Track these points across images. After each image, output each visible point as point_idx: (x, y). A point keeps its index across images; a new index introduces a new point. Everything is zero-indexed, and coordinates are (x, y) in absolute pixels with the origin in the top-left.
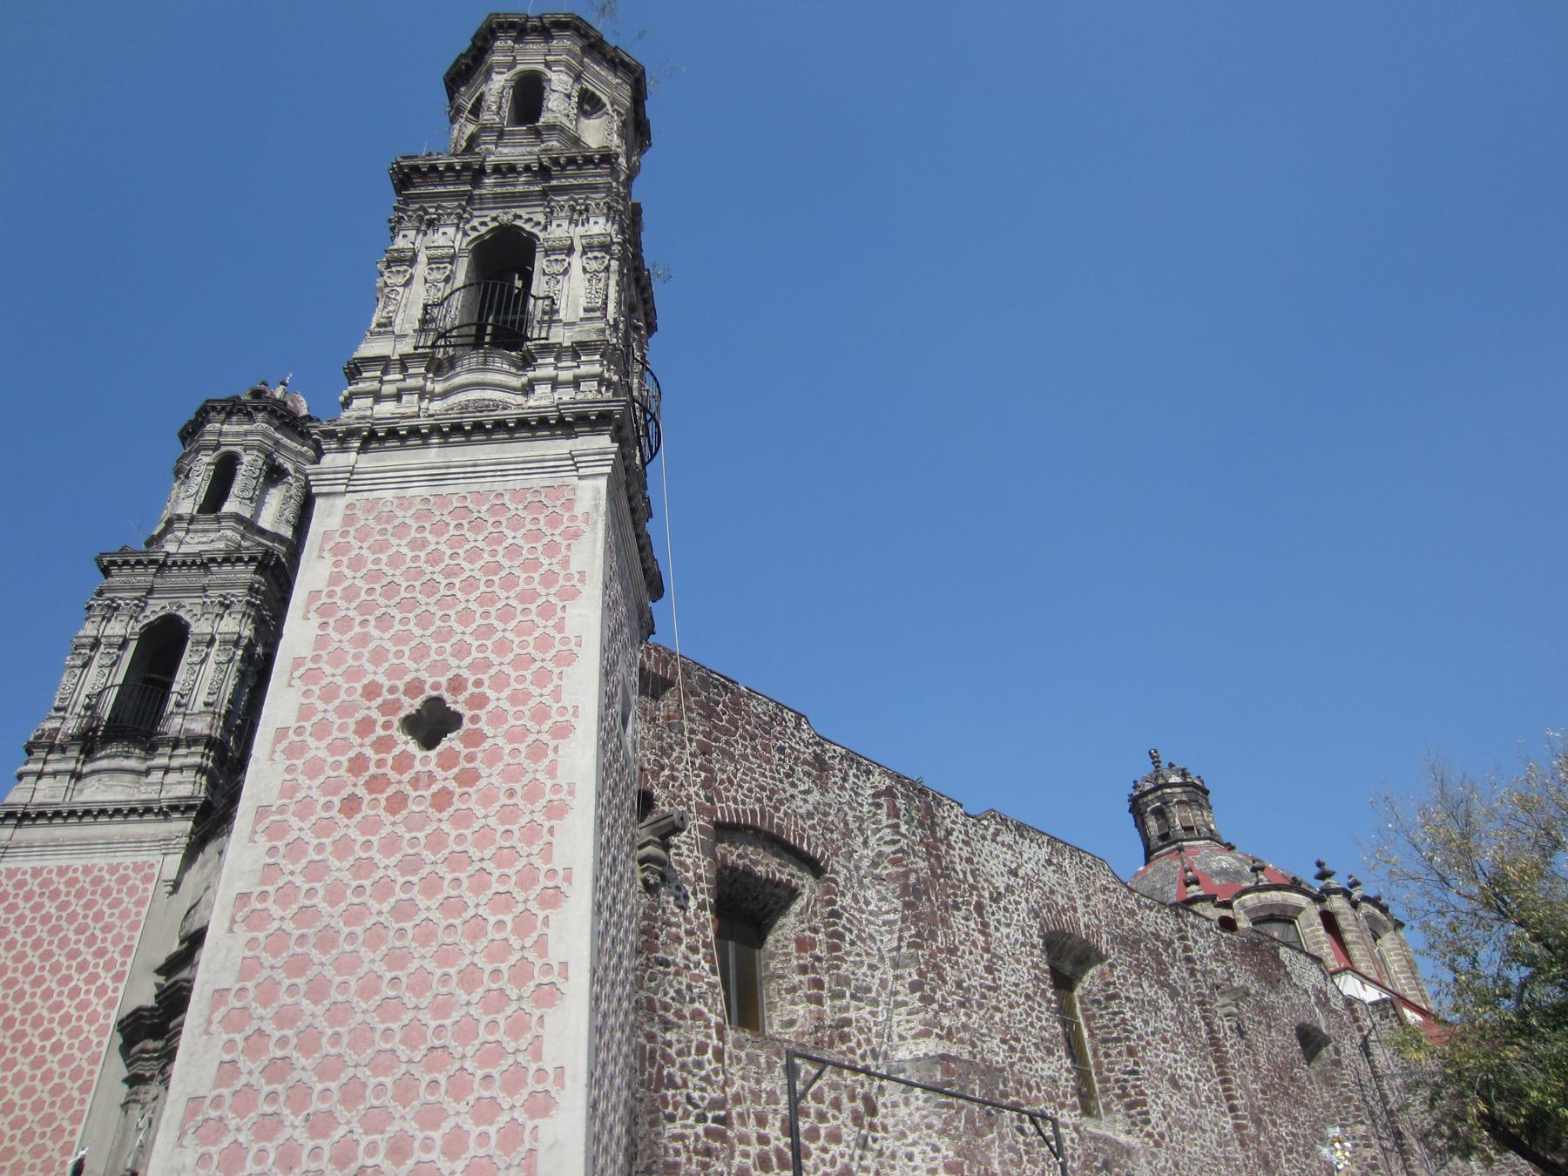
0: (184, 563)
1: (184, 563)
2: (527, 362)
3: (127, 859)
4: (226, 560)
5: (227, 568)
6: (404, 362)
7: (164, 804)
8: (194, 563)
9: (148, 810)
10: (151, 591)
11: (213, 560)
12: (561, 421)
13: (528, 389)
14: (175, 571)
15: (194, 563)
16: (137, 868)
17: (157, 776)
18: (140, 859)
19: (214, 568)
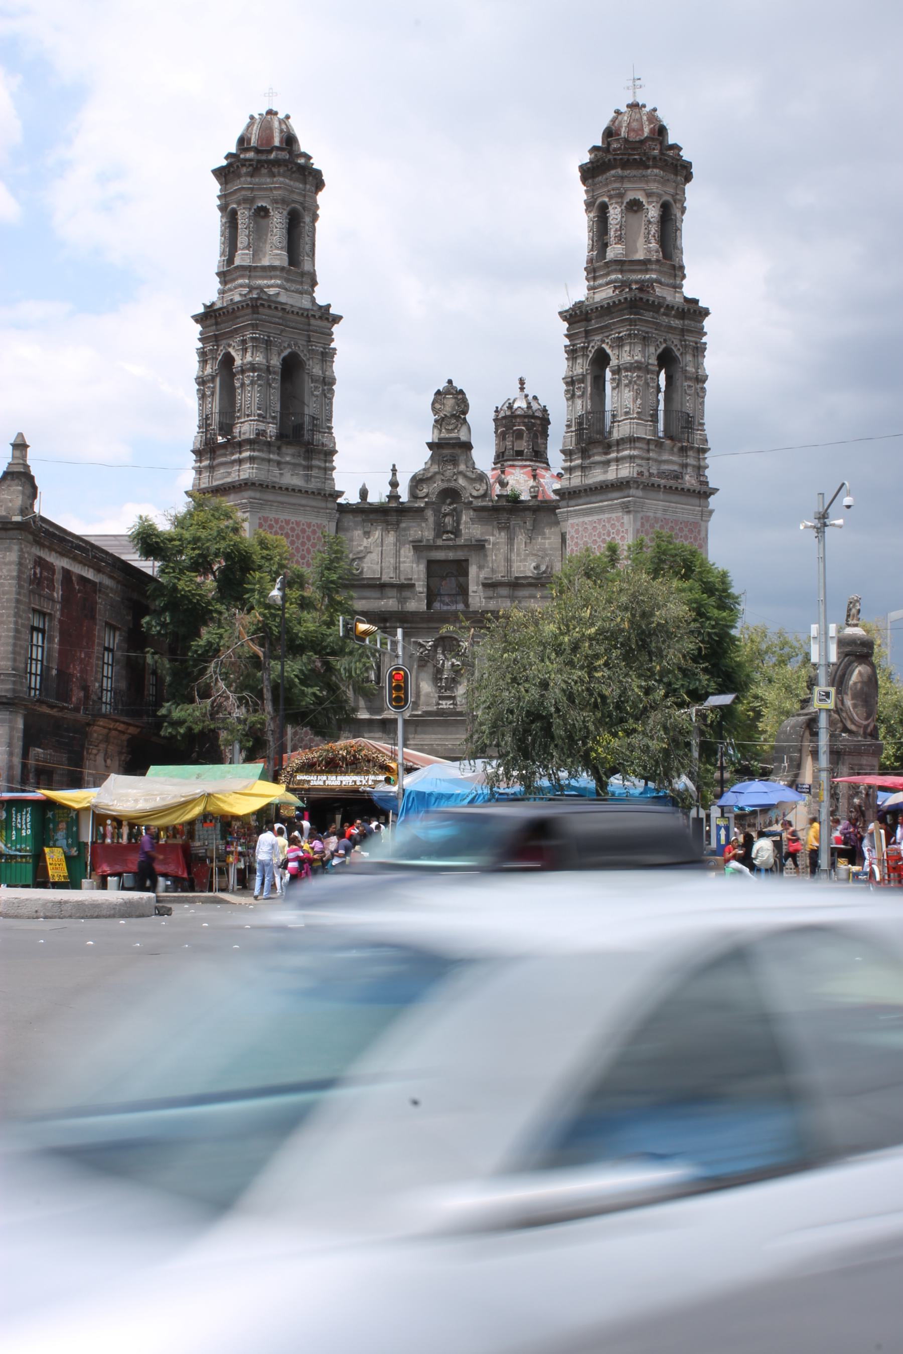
0: (298, 313)
1: (298, 313)
2: (683, 450)
3: (315, 521)
4: (320, 318)
5: (319, 323)
6: (649, 442)
7: (327, 493)
8: (302, 314)
9: (319, 494)
10: (282, 331)
11: (314, 316)
12: (699, 492)
13: (685, 466)
14: (290, 316)
15: (302, 314)
16: (319, 526)
17: (314, 472)
18: (319, 522)
19: (313, 321)
